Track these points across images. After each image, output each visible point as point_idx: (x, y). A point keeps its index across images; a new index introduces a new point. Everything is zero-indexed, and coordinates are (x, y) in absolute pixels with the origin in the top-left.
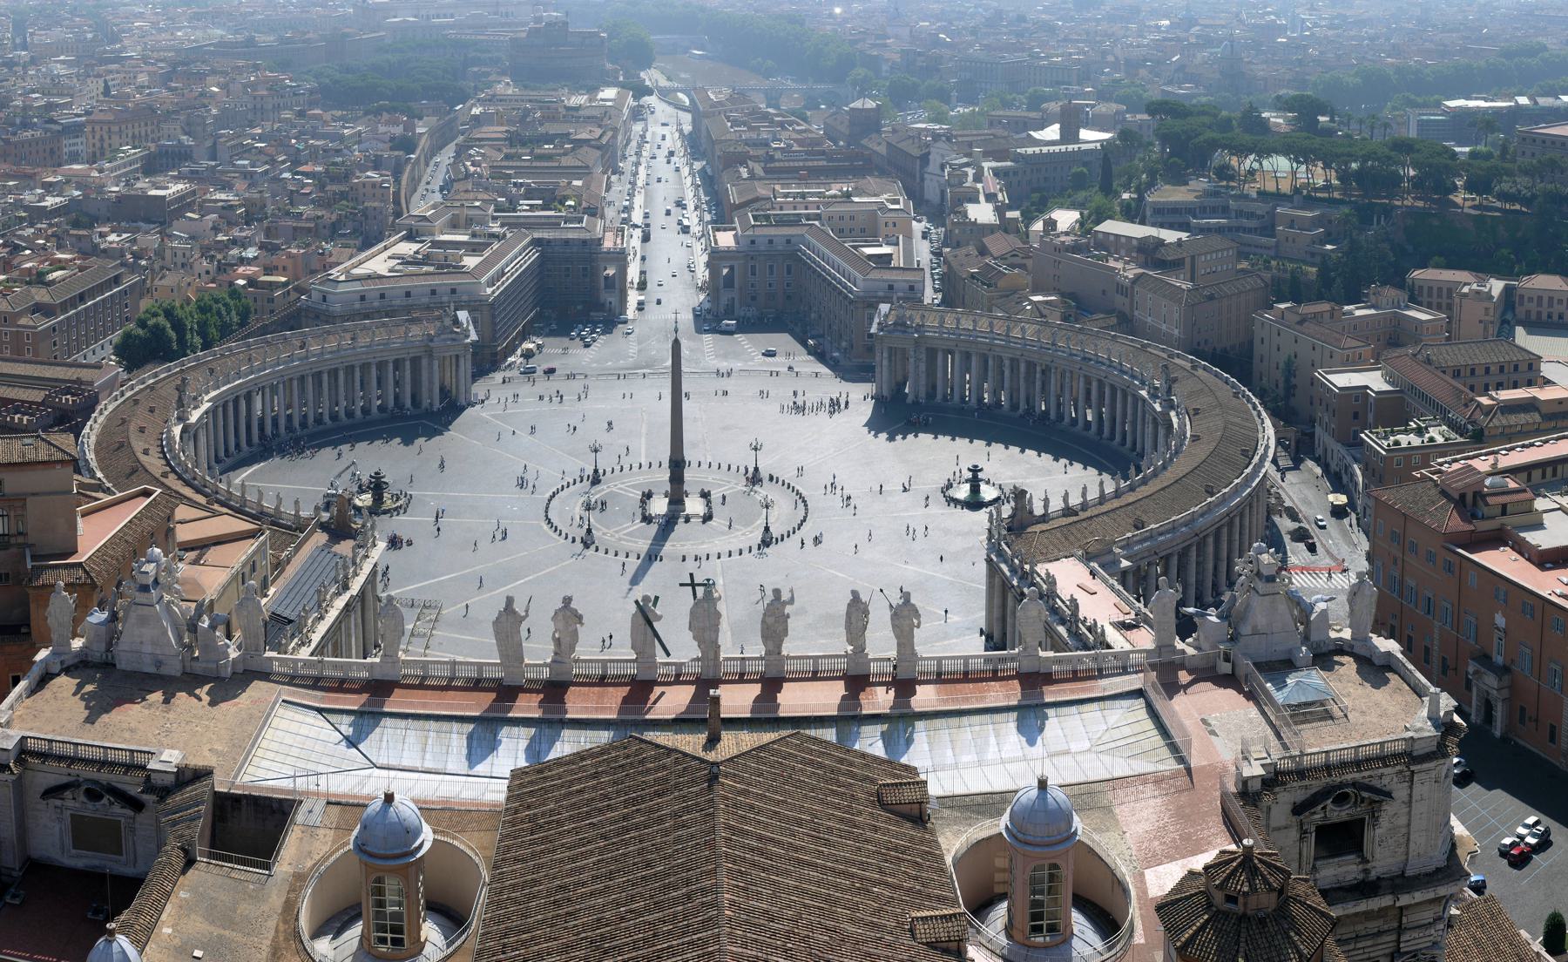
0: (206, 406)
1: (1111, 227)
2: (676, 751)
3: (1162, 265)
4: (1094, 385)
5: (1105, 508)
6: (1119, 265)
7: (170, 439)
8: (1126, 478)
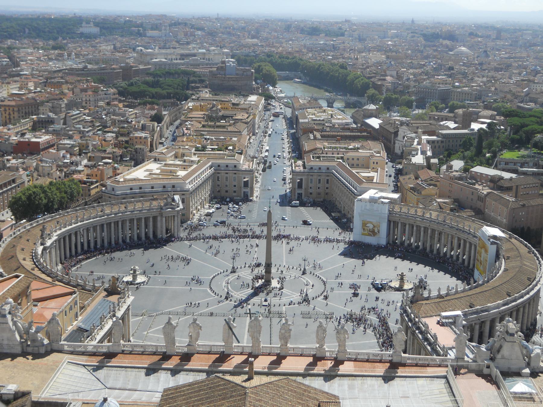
0: (54, 238)
1: (479, 169)
2: (233, 382)
3: (501, 189)
4: (462, 242)
5: (457, 296)
6: (480, 187)
7: (36, 253)
8: (468, 284)
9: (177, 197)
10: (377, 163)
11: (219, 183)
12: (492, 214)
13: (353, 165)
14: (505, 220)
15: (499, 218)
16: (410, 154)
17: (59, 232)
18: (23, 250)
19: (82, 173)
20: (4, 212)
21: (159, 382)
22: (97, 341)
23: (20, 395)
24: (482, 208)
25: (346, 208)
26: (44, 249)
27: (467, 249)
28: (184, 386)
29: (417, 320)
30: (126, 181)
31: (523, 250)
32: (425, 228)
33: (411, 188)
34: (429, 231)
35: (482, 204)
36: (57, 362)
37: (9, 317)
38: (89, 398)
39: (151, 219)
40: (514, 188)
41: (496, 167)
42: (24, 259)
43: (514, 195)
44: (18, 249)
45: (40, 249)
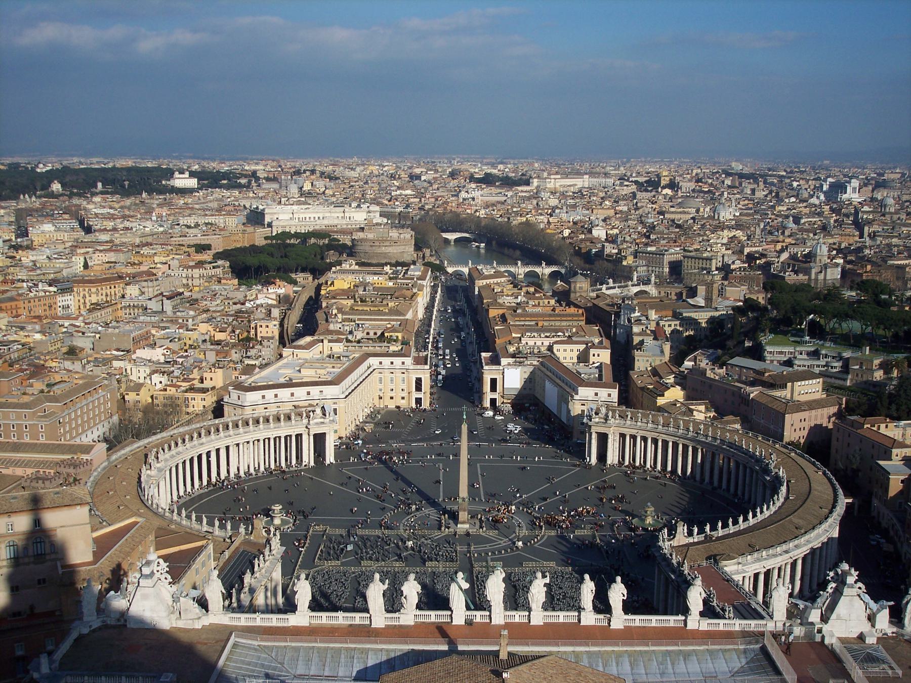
1: (738, 361)
3: (772, 386)
12: (762, 421)
13: (565, 358)
15: (772, 427)
20: (89, 433)
27: (733, 472)
31: (810, 469)
34: (680, 447)
39: (294, 439)
40: (789, 384)
43: (789, 396)
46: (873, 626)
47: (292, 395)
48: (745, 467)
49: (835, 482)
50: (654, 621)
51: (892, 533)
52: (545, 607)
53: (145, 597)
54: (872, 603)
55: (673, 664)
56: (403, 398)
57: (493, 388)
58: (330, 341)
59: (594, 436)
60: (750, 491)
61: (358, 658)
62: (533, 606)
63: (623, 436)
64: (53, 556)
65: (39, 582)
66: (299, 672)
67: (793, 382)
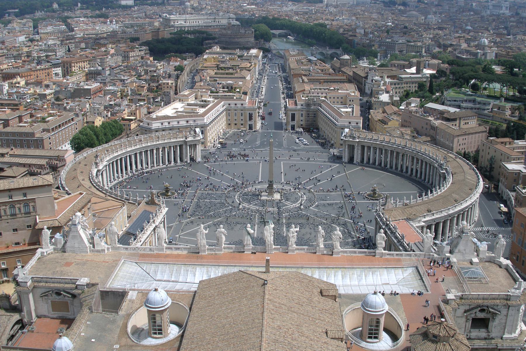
0: (105, 163)
1: (431, 105)
3: (448, 120)
4: (420, 161)
9: (198, 130)
10: (353, 101)
11: (229, 118)
12: (442, 139)
13: (334, 102)
14: (451, 145)
15: (447, 142)
16: (378, 93)
17: (108, 159)
18: (82, 172)
19: (124, 112)
20: (67, 144)
21: (195, 276)
22: (142, 242)
23: (90, 286)
24: (434, 135)
25: (330, 136)
26: (98, 171)
27: (424, 167)
28: (216, 278)
29: (388, 222)
30: (158, 118)
31: (466, 167)
32: (391, 151)
33: (379, 120)
35: (434, 132)
36: (116, 261)
37: (79, 227)
38: (142, 288)
40: (458, 119)
41: (443, 104)
42: (83, 180)
43: (458, 125)
44: (78, 171)
45: (94, 171)
46: (478, 255)
47: (178, 122)
48: (430, 166)
49: (479, 174)
50: (357, 252)
51: (508, 203)
52: (297, 244)
53: (74, 237)
54: (479, 243)
55: (366, 276)
56: (242, 124)
57: (293, 119)
58: (201, 92)
59: (347, 147)
60: (432, 179)
61: (191, 271)
62: (290, 243)
63: (363, 147)
64: (34, 214)
65: (28, 226)
66: (157, 278)
67: (460, 118)
